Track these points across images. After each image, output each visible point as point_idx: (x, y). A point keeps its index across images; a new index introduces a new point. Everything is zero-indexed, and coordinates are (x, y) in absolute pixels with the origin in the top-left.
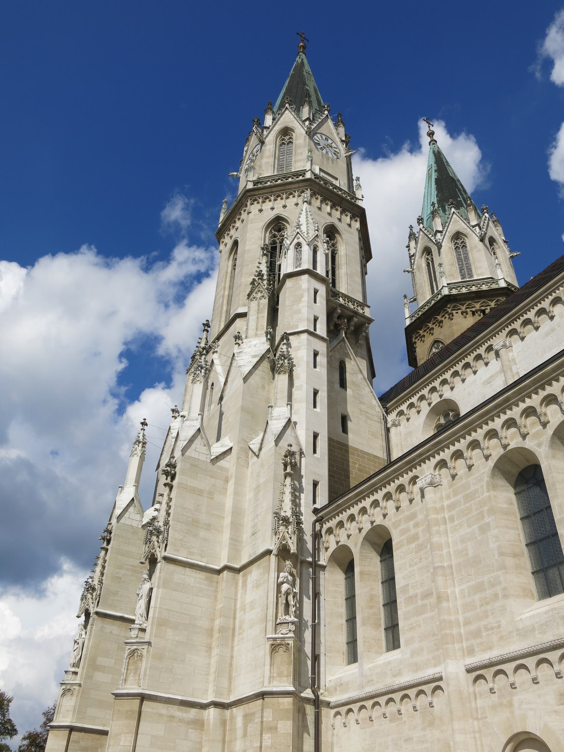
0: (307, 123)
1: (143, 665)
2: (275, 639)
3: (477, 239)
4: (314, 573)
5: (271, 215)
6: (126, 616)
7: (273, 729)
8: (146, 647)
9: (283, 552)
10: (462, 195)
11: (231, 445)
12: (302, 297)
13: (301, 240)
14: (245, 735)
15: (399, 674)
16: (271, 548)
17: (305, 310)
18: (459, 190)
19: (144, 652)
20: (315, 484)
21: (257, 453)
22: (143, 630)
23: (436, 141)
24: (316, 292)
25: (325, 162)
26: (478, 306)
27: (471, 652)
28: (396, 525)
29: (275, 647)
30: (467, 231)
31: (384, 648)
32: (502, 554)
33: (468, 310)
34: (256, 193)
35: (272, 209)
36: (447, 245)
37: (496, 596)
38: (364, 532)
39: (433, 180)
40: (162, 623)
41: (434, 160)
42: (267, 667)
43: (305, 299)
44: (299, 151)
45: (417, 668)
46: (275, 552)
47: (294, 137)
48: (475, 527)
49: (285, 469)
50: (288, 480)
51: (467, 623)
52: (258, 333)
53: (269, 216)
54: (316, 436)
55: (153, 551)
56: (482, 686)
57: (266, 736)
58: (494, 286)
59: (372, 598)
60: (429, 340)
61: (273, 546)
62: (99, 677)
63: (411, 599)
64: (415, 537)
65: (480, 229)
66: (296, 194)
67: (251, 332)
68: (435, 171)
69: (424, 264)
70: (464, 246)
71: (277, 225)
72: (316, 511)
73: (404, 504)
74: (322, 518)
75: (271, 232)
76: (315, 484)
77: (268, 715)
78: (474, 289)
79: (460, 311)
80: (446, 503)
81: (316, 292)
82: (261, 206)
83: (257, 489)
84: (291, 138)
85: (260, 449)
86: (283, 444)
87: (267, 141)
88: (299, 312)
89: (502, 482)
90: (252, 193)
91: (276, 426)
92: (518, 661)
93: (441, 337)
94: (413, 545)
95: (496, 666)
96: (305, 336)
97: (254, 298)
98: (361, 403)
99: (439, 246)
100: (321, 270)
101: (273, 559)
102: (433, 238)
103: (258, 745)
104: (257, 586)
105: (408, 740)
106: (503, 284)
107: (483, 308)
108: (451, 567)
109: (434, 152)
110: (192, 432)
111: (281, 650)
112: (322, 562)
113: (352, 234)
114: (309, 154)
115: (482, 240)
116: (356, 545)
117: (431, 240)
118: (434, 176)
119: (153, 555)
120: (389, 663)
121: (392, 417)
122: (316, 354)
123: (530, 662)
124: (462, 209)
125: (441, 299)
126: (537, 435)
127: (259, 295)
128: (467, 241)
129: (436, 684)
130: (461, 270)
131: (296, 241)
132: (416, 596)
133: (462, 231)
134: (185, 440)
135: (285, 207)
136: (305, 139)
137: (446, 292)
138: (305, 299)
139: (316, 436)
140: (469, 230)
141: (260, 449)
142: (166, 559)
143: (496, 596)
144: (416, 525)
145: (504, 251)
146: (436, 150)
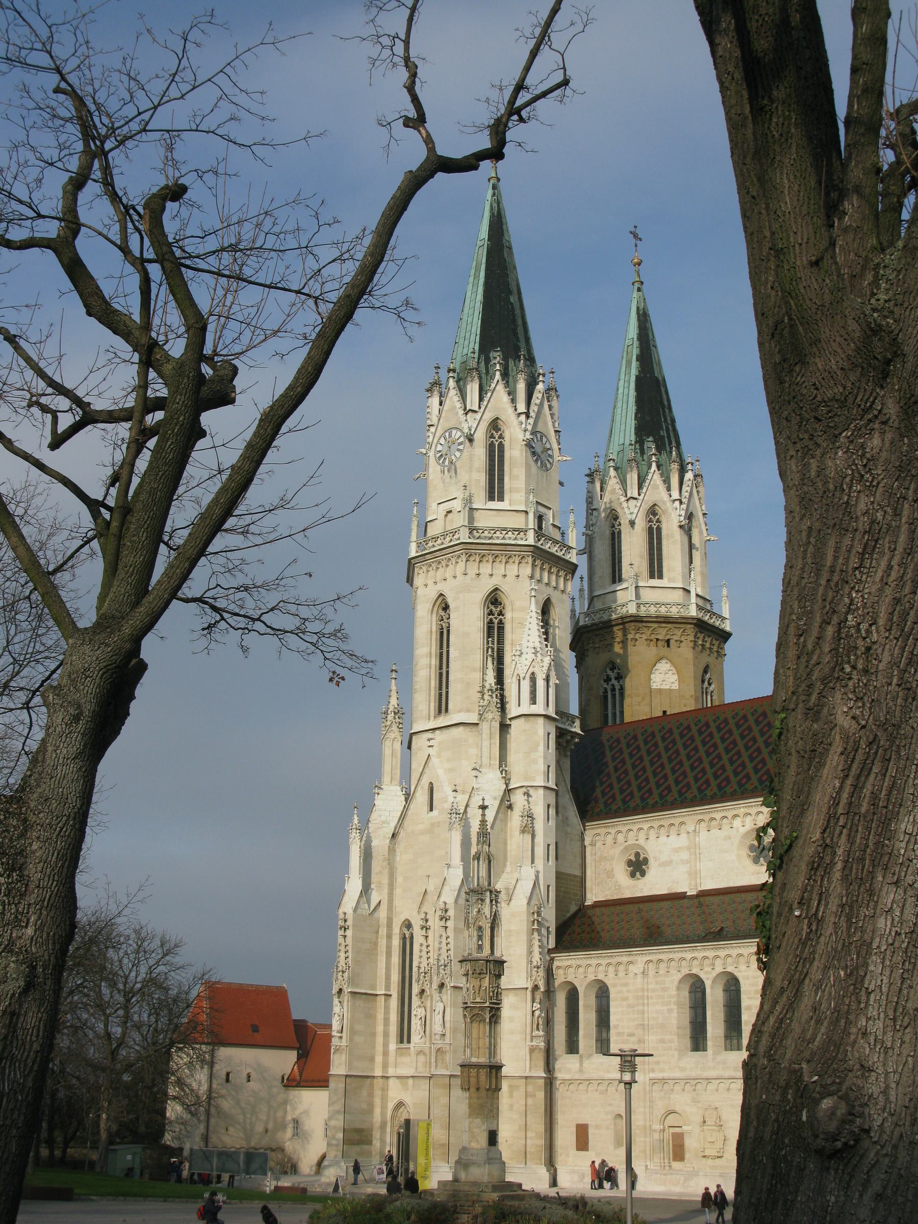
3: (675, 524)
6: (369, 992)
10: (666, 421)
13: (536, 670)
14: (511, 1096)
15: (608, 1072)
17: (541, 761)
18: (663, 407)
27: (653, 1071)
28: (615, 986)
29: (532, 1050)
32: (678, 1028)
33: (653, 637)
34: (473, 547)
36: (641, 524)
39: (633, 378)
42: (528, 1062)
43: (541, 748)
44: (515, 472)
47: (507, 435)
48: (665, 1008)
53: (487, 586)
54: (548, 886)
56: (656, 1087)
57: (530, 1101)
60: (604, 657)
61: (530, 985)
62: (358, 1039)
63: (619, 1034)
64: (626, 999)
65: (681, 503)
67: (485, 760)
68: (637, 360)
69: (608, 533)
70: (659, 529)
73: (621, 974)
78: (663, 610)
79: (644, 637)
89: (682, 986)
90: (468, 546)
91: (526, 887)
92: (676, 1080)
94: (625, 1003)
95: (664, 1081)
98: (568, 825)
99: (632, 523)
100: (551, 712)
101: (529, 993)
102: (625, 505)
105: (610, 1105)
106: (693, 612)
107: (668, 637)
115: (681, 527)
122: (549, 806)
123: (683, 1082)
124: (664, 456)
126: (707, 973)
127: (490, 716)
128: (663, 519)
135: (505, 576)
136: (522, 450)
139: (548, 886)
140: (669, 504)
144: (628, 991)
145: (701, 532)
146: (641, 307)
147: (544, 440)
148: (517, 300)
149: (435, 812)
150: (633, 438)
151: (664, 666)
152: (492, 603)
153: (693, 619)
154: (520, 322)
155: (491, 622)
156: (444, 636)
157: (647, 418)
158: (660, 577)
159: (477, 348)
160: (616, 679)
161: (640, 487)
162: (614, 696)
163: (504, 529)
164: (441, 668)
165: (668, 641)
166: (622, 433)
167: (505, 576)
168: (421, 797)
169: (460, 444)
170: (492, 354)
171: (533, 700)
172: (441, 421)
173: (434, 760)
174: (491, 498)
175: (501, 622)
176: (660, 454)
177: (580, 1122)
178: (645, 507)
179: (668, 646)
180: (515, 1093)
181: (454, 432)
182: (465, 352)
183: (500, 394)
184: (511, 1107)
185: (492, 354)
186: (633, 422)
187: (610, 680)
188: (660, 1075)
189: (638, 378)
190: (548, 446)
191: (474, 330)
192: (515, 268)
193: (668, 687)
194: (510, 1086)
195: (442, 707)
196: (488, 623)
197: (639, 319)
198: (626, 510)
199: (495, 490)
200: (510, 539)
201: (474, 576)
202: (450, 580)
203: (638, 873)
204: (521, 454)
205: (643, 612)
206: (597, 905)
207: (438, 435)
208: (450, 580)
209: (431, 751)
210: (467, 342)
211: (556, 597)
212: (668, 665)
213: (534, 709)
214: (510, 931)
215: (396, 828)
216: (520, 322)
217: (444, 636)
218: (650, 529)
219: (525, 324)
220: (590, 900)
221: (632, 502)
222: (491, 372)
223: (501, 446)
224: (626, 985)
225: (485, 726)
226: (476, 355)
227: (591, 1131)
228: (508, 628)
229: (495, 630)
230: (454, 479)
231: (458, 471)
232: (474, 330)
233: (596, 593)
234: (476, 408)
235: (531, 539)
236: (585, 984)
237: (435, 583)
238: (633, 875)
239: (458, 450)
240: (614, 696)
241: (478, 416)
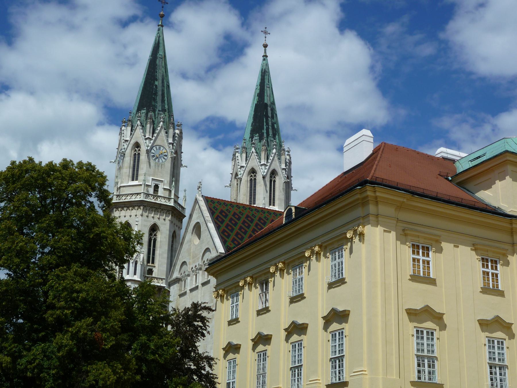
0: (147, 141)
10: (267, 124)
18: (267, 117)
23: (267, 56)
25: (157, 170)
35: (125, 216)
66: (136, 208)
87: (126, 153)
109: (262, 69)
113: (165, 224)
147: (162, 148)
148: (160, 81)
154: (160, 93)
167: (130, 216)
174: (133, 180)
178: (248, 169)
183: (139, 131)
189: (256, 105)
190: (164, 151)
199: (135, 176)
211: (159, 223)
223: (139, 154)
241: (128, 143)
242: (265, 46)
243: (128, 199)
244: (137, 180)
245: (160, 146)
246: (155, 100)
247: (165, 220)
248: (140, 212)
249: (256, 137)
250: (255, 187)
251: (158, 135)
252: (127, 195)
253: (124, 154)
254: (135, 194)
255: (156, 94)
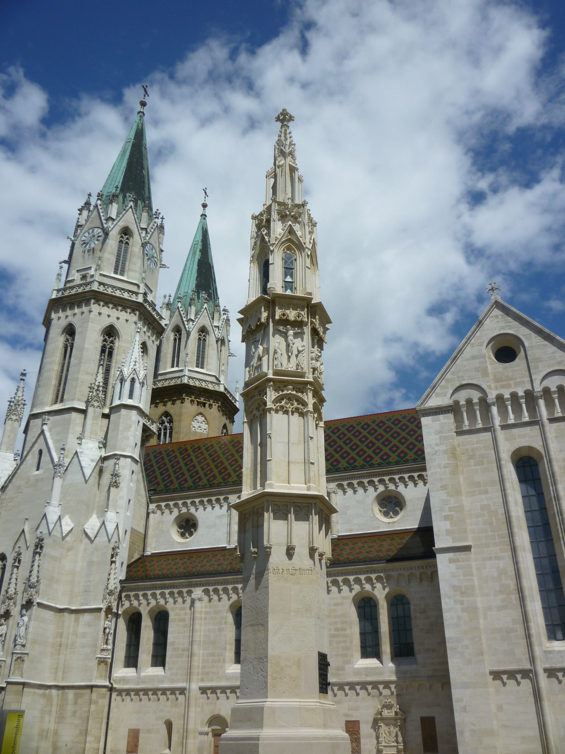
1: (26, 665)
2: (101, 658)
3: (215, 339)
4: (117, 620)
5: (106, 322)
7: (96, 703)
8: (26, 656)
9: (109, 610)
11: (72, 525)
12: (131, 427)
13: (135, 376)
14: (75, 703)
15: (162, 682)
16: (101, 606)
17: (131, 438)
18: (212, 279)
19: (25, 659)
20: (122, 563)
21: (93, 539)
22: (24, 646)
23: (206, 216)
24: (139, 422)
26: (202, 400)
27: (202, 680)
30: (210, 328)
31: (150, 665)
36: (194, 335)
37: (219, 660)
38: (151, 606)
39: (197, 260)
40: (34, 642)
41: (201, 238)
44: (134, 260)
45: (173, 681)
46: (104, 609)
49: (112, 558)
50: (113, 564)
51: (203, 668)
52: (92, 436)
54: (126, 531)
55: (31, 597)
57: (93, 707)
58: (217, 388)
59: (149, 639)
61: (103, 606)
64: (184, 620)
70: (204, 340)
71: (110, 332)
72: (121, 581)
74: (124, 587)
75: (104, 337)
76: (122, 563)
77: (94, 696)
78: (204, 385)
79: (190, 399)
80: (204, 610)
81: (139, 422)
82: (100, 309)
83: (90, 564)
84: (127, 239)
85: (95, 537)
86: (113, 540)
87: (111, 234)
88: (127, 438)
91: (111, 527)
92: (223, 690)
93: (172, 412)
95: (214, 690)
96: (129, 460)
97: (93, 405)
98: (139, 495)
99: (188, 333)
101: (103, 614)
102: (186, 323)
103: (87, 709)
104: (89, 625)
106: (222, 389)
108: (200, 641)
110: (56, 518)
111: (103, 664)
112: (120, 612)
114: (144, 275)
115: (217, 342)
116: (145, 610)
117: (183, 322)
118: (198, 256)
119: (30, 600)
120: (157, 676)
121: (152, 506)
124: (211, 303)
125: (180, 385)
127: (96, 404)
128: (207, 336)
129: (182, 691)
130: (198, 360)
131: (132, 376)
132: (179, 648)
133: (207, 326)
134: (52, 524)
136: (140, 249)
137: (185, 380)
138: (132, 429)
139: (126, 531)
141: (95, 537)
142: (38, 603)
143: (219, 660)
144: (185, 614)
149: (41, 471)
150: (194, 287)
151: (200, 418)
152: (107, 335)
153: (221, 393)
155: (104, 347)
156: (68, 349)
157: (203, 281)
158: (202, 368)
159: (120, 186)
160: (168, 423)
161: (196, 314)
162: (165, 434)
163: (123, 289)
164: (62, 372)
165: (204, 405)
166: (187, 287)
168: (32, 459)
169: (99, 237)
170: (128, 195)
171: (131, 396)
172: (88, 223)
173: (47, 434)
174: (116, 272)
175: (111, 348)
176: (209, 301)
177: (133, 727)
178: (198, 326)
179: (204, 406)
180: (79, 701)
181: (96, 229)
182: (110, 190)
184: (75, 712)
185: (128, 195)
186: (195, 282)
187: (164, 423)
188: (209, 684)
189: (199, 260)
190: (155, 256)
191: (118, 180)
192: (147, 159)
193: (200, 431)
194: (76, 694)
195: (59, 397)
196: (102, 347)
197: (203, 232)
198: (187, 326)
199: (120, 267)
200: (126, 296)
201: (97, 314)
202: (79, 315)
203: (187, 535)
204: (140, 251)
205: (191, 383)
206: (153, 555)
207: (84, 231)
208: (79, 315)
209: (45, 427)
210: (112, 186)
212: (203, 418)
213: (130, 402)
214: (92, 562)
215: (5, 482)
216: (147, 186)
217: (68, 349)
218: (199, 339)
219: (149, 189)
220: (148, 553)
221: (191, 323)
222: (126, 203)
224: (184, 609)
225: (91, 410)
226: (118, 191)
227: (141, 735)
228: (115, 352)
229: (107, 352)
230: (91, 256)
231: (95, 252)
232: (118, 180)
233: (160, 372)
234: (114, 217)
235: (140, 299)
236: (149, 608)
237: (67, 317)
238: (183, 535)
239: (97, 240)
240: (165, 434)
242: (204, 206)
243: (118, 293)
244: (122, 274)
245: (153, 247)
246: (144, 190)
247: (153, 341)
248: (134, 318)
249: (204, 295)
250: (204, 348)
251: (153, 233)
252: (113, 287)
253: (106, 234)
254: (129, 291)
255: (144, 182)
